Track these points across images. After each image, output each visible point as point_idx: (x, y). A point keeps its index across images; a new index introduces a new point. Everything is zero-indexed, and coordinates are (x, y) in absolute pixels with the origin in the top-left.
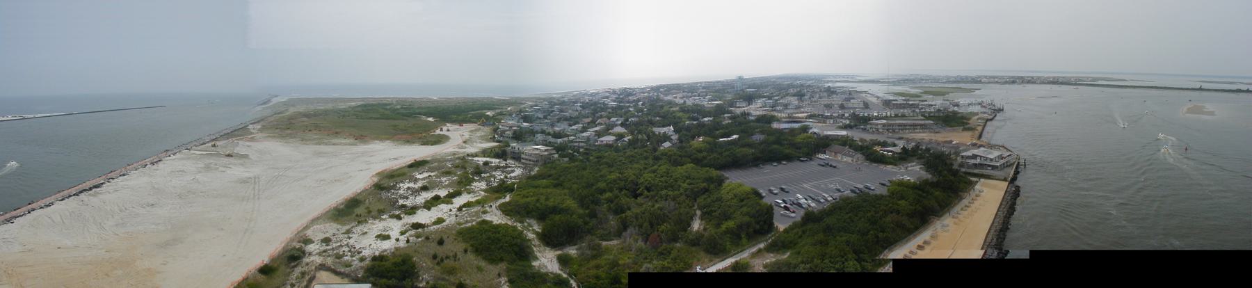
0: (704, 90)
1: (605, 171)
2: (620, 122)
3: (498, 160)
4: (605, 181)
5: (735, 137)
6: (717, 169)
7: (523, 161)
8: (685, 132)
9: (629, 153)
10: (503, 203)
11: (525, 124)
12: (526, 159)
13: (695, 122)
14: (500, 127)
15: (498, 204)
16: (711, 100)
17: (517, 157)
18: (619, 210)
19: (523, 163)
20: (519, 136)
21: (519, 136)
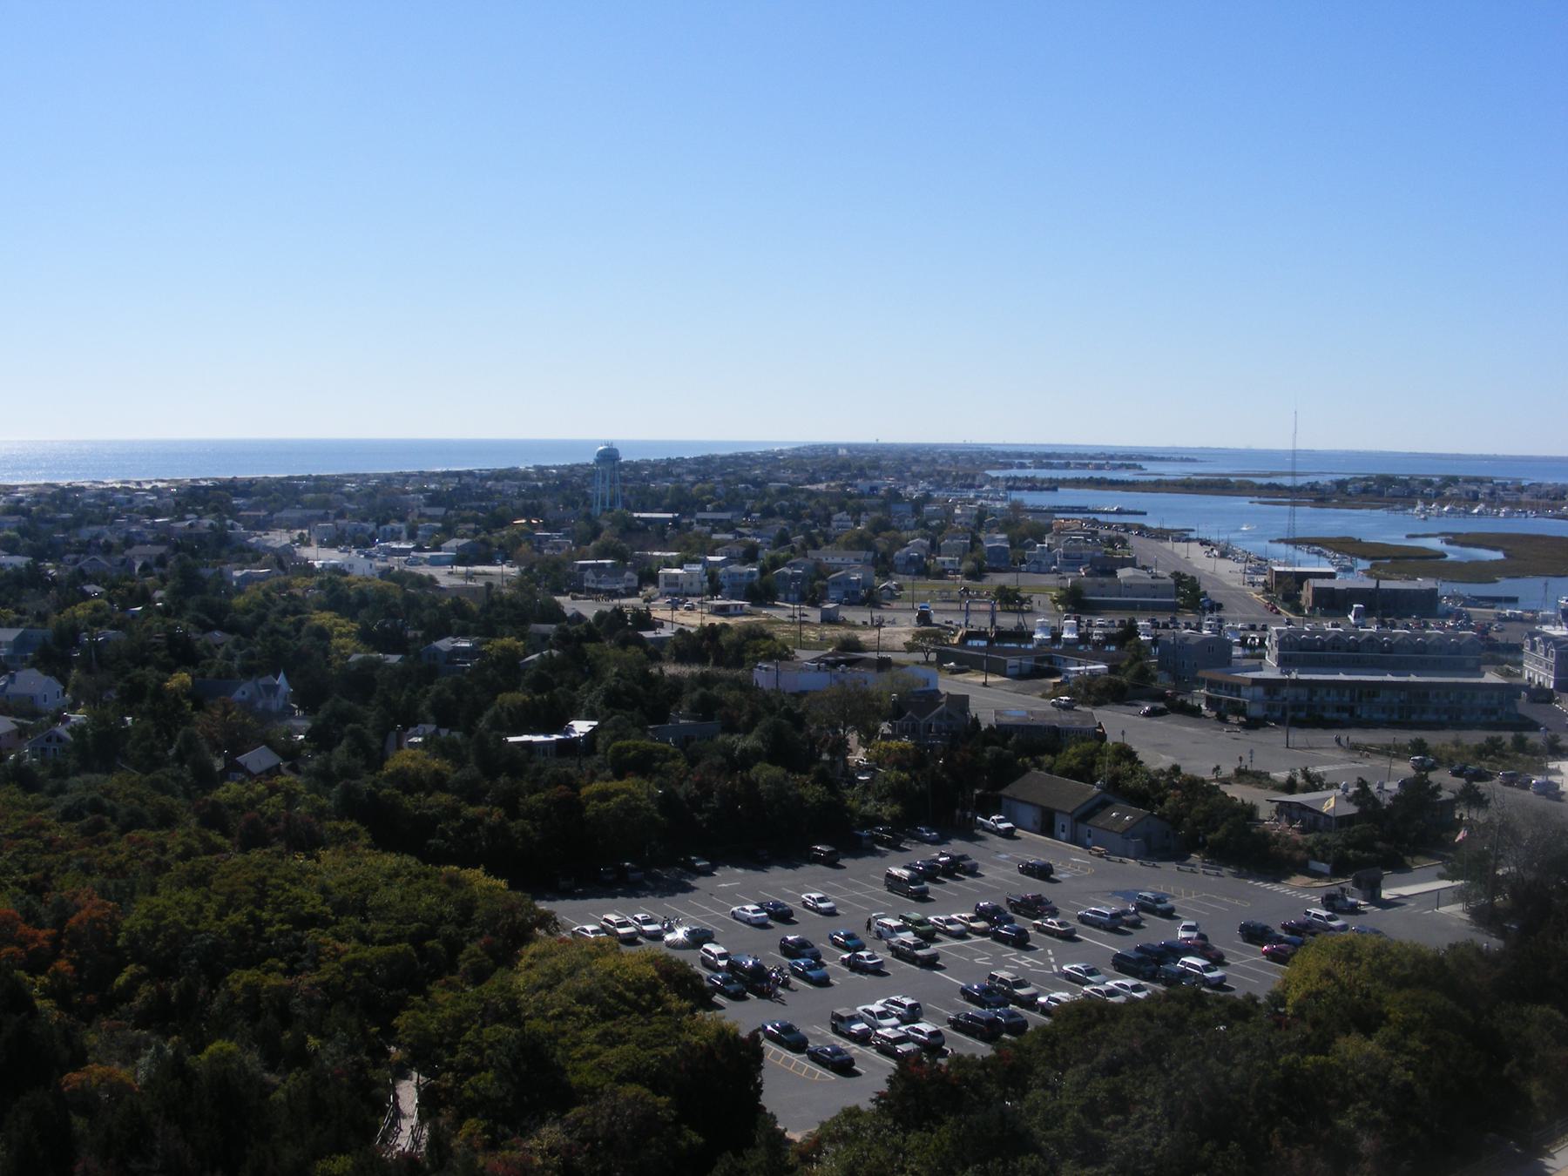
0: (440, 511)
5: (581, 727)
9: (81, 786)
13: (394, 659)
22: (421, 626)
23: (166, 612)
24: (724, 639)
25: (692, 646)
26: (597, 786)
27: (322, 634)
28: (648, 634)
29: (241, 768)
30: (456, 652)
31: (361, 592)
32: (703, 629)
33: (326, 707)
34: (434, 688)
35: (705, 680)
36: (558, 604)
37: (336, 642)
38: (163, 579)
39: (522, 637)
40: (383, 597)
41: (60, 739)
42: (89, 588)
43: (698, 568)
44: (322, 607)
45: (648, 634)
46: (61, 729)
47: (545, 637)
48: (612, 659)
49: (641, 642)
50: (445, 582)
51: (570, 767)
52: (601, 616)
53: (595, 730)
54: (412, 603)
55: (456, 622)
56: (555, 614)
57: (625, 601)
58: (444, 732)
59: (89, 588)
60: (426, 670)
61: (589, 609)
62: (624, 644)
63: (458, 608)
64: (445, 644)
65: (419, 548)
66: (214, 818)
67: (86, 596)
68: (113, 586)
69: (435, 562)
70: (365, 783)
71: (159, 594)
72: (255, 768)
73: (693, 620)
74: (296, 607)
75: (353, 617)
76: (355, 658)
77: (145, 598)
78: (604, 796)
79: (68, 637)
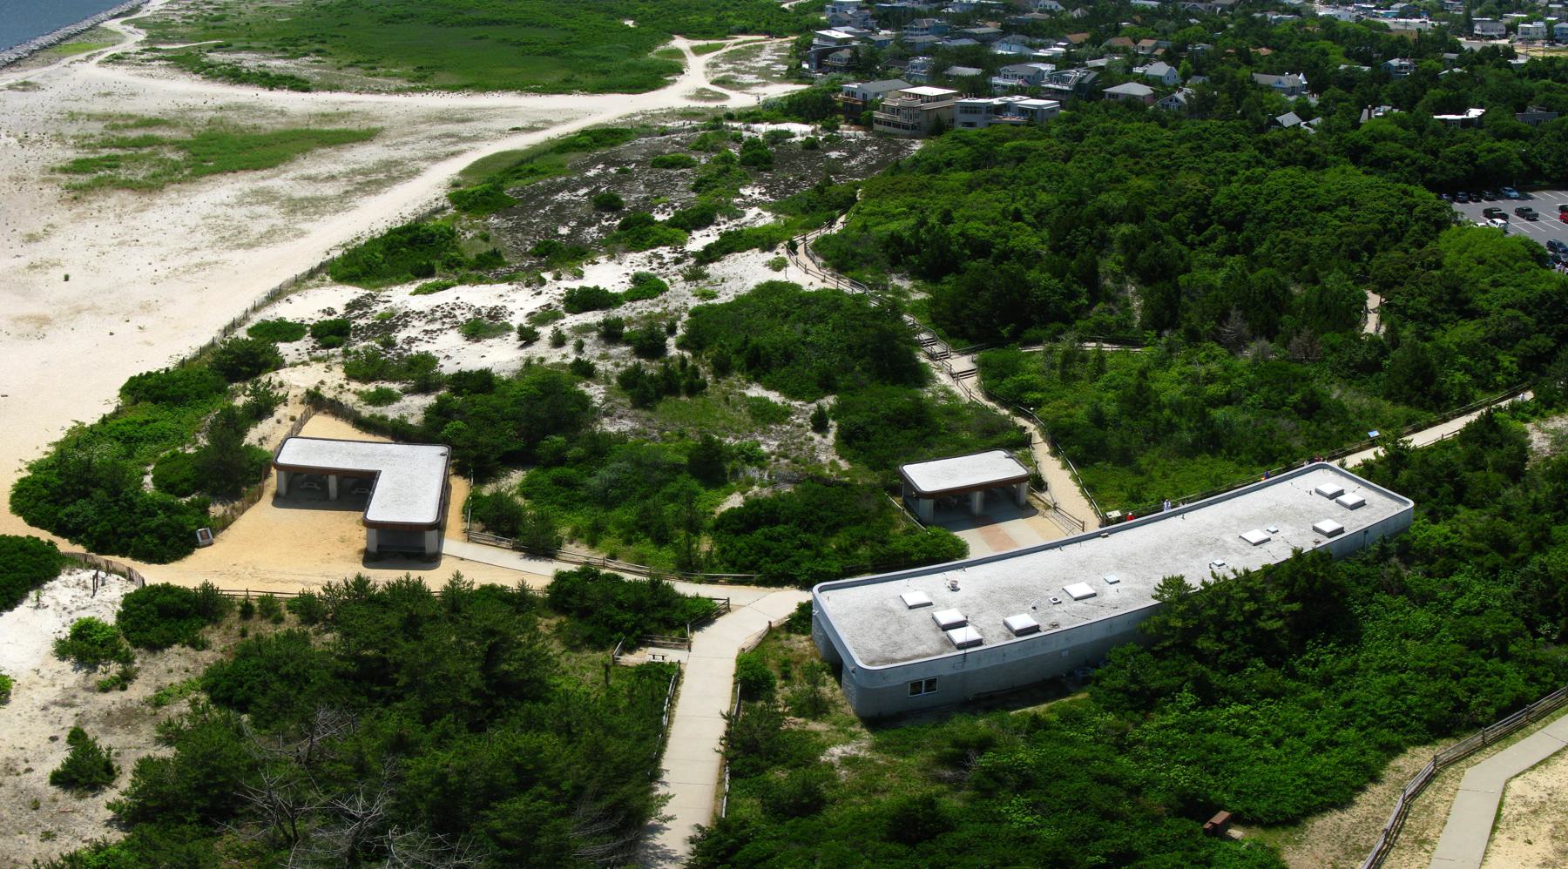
1: (1120, 166)
2: (1159, 52)
3: (807, 128)
4: (1125, 191)
5: (1474, 113)
6: (1431, 186)
7: (877, 127)
8: (1339, 92)
10: (825, 239)
11: (883, 32)
12: (888, 123)
13: (1366, 69)
14: (816, 41)
15: (812, 236)
16: (1402, 15)
17: (858, 113)
18: (1156, 274)
19: (881, 135)
20: (864, 64)
21: (864, 64)
22: (1380, 51)
23: (1235, 36)
24: (1558, 65)
25: (1536, 70)
26: (1485, 145)
27: (1324, 53)
28: (1513, 62)
29: (1278, 123)
30: (1401, 67)
31: (1346, 30)
32: (1544, 58)
33: (1327, 94)
34: (1390, 86)
35: (1548, 88)
36: (1459, 43)
37: (1331, 57)
38: (1233, 18)
39: (1439, 61)
40: (1357, 34)
41: (1177, 101)
42: (1192, 21)
43: (1540, 24)
44: (1326, 38)
45: (1513, 62)
46: (1180, 96)
47: (1451, 60)
48: (1489, 72)
49: (1509, 66)
50: (1392, 27)
51: (1469, 133)
52: (1484, 49)
53: (1484, 114)
54: (1374, 38)
55: (1401, 50)
56: (1456, 48)
57: (1498, 42)
58: (1396, 111)
59: (1192, 21)
60: (1386, 76)
61: (1477, 45)
62: (1499, 66)
63: (1402, 41)
64: (1395, 62)
65: (1378, 8)
66: (1267, 148)
67: (1191, 25)
68: (1204, 20)
69: (1385, 16)
70: (1353, 135)
71: (1230, 26)
72: (1286, 124)
73: (1539, 51)
74: (1309, 37)
75: (1342, 44)
76: (1342, 67)
77: (1223, 27)
78: (1491, 151)
79: (1181, 47)
